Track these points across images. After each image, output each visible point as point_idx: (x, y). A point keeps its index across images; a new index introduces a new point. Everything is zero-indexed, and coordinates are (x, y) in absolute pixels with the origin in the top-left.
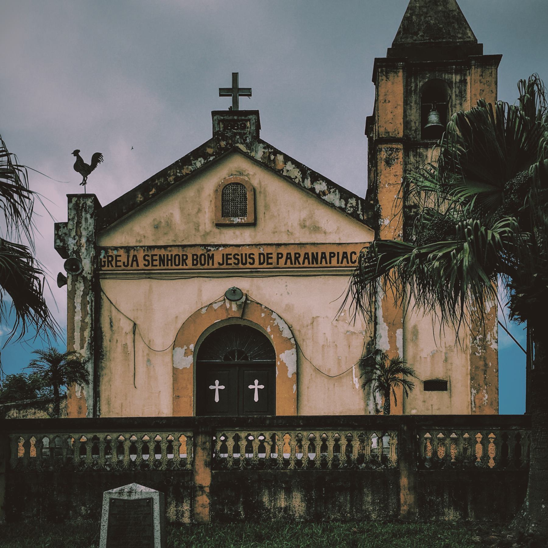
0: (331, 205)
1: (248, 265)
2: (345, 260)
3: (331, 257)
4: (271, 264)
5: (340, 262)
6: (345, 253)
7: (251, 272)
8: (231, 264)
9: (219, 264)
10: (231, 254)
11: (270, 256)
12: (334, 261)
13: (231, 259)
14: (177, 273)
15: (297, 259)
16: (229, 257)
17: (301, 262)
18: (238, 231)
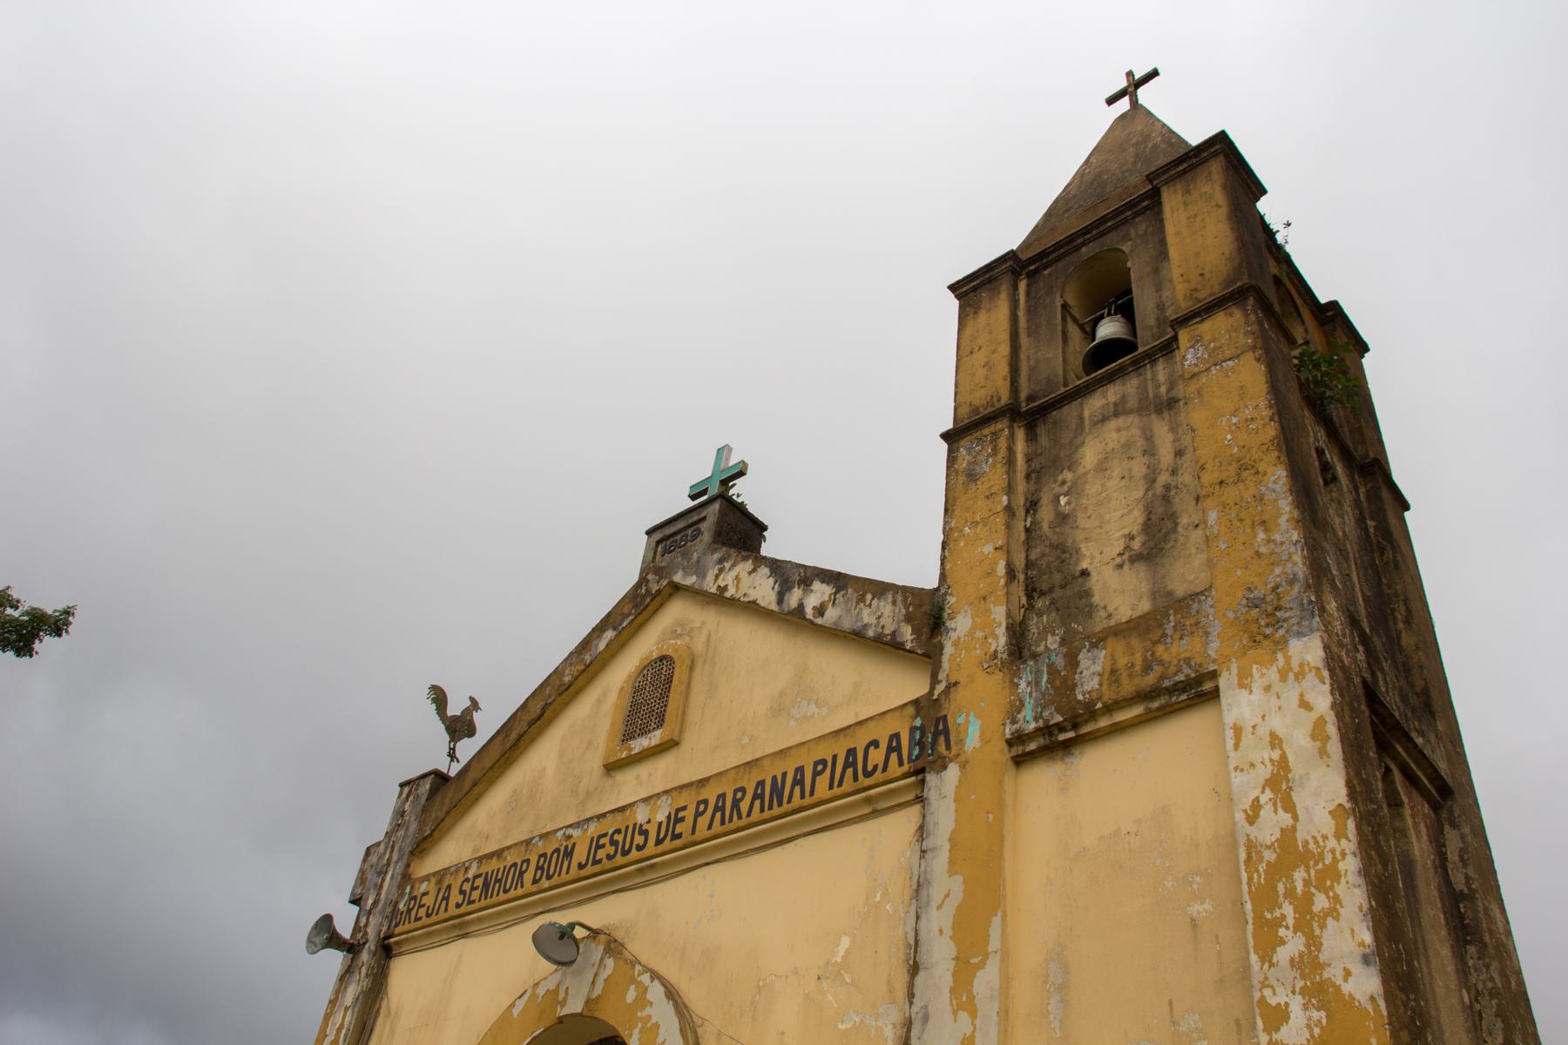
0: (834, 634)
1: (635, 854)
2: (850, 771)
3: (816, 774)
4: (679, 836)
5: (836, 783)
6: (852, 752)
7: (641, 870)
8: (600, 861)
9: (580, 864)
10: (605, 835)
11: (681, 815)
12: (823, 781)
13: (603, 846)
14: (507, 911)
15: (736, 804)
16: (602, 841)
17: (744, 811)
18: (642, 770)
